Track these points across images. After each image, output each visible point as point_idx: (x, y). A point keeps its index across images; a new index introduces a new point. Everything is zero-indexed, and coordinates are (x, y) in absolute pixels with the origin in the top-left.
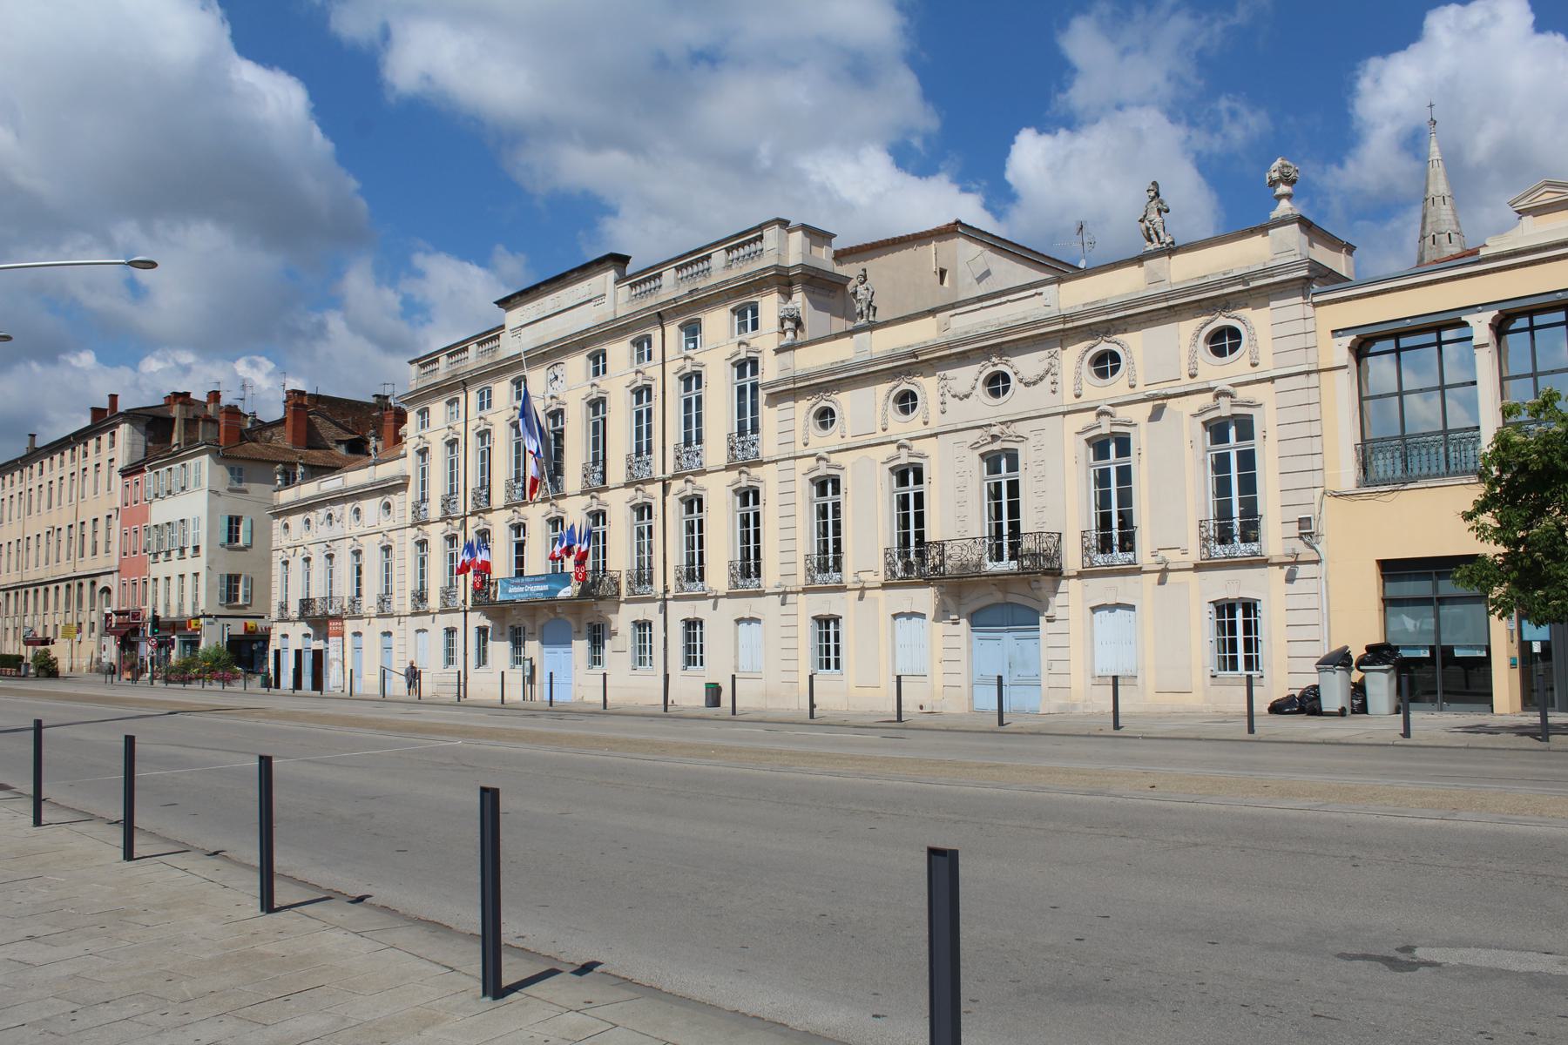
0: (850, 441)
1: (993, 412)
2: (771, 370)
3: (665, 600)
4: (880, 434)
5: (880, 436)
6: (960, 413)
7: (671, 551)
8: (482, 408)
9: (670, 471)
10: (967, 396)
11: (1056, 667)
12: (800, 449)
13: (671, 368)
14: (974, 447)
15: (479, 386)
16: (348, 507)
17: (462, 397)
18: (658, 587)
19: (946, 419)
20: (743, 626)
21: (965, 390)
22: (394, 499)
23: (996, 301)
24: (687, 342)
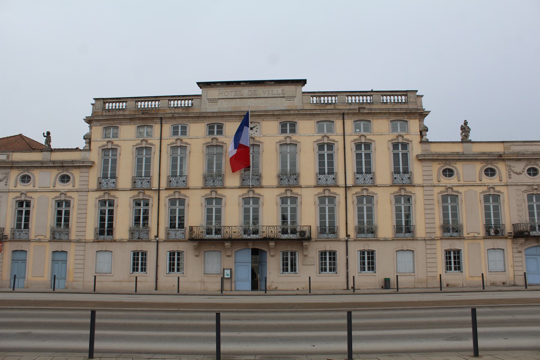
0: (462, 182)
1: (532, 181)
2: (416, 149)
3: (347, 241)
4: (478, 182)
6: (515, 178)
7: (347, 219)
8: (175, 133)
9: (350, 183)
10: (521, 174)
12: (435, 182)
13: (348, 139)
14: (525, 191)
15: (175, 122)
16: (15, 174)
17: (157, 127)
18: (342, 235)
19: (510, 181)
20: (400, 255)
21: (518, 171)
22: (76, 174)
23: (530, 144)
24: (356, 128)
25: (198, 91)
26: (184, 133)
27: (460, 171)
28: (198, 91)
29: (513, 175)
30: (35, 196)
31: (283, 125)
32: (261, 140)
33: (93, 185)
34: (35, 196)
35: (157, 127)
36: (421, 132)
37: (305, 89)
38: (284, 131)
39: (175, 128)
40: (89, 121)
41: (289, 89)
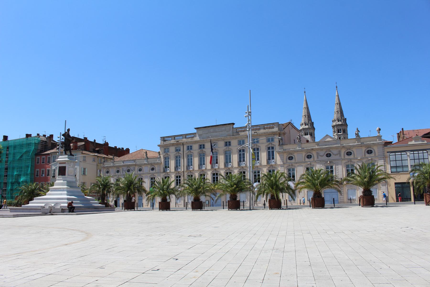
4: (304, 161)
5: (304, 161)
8: (188, 149)
11: (341, 198)
25: (195, 131)
26: (191, 149)
27: (296, 157)
28: (195, 131)
29: (319, 157)
30: (144, 175)
31: (226, 143)
32: (218, 149)
33: (162, 171)
34: (144, 175)
35: (182, 147)
36: (279, 141)
37: (235, 126)
38: (226, 145)
39: (188, 147)
40: (159, 146)
41: (228, 127)
